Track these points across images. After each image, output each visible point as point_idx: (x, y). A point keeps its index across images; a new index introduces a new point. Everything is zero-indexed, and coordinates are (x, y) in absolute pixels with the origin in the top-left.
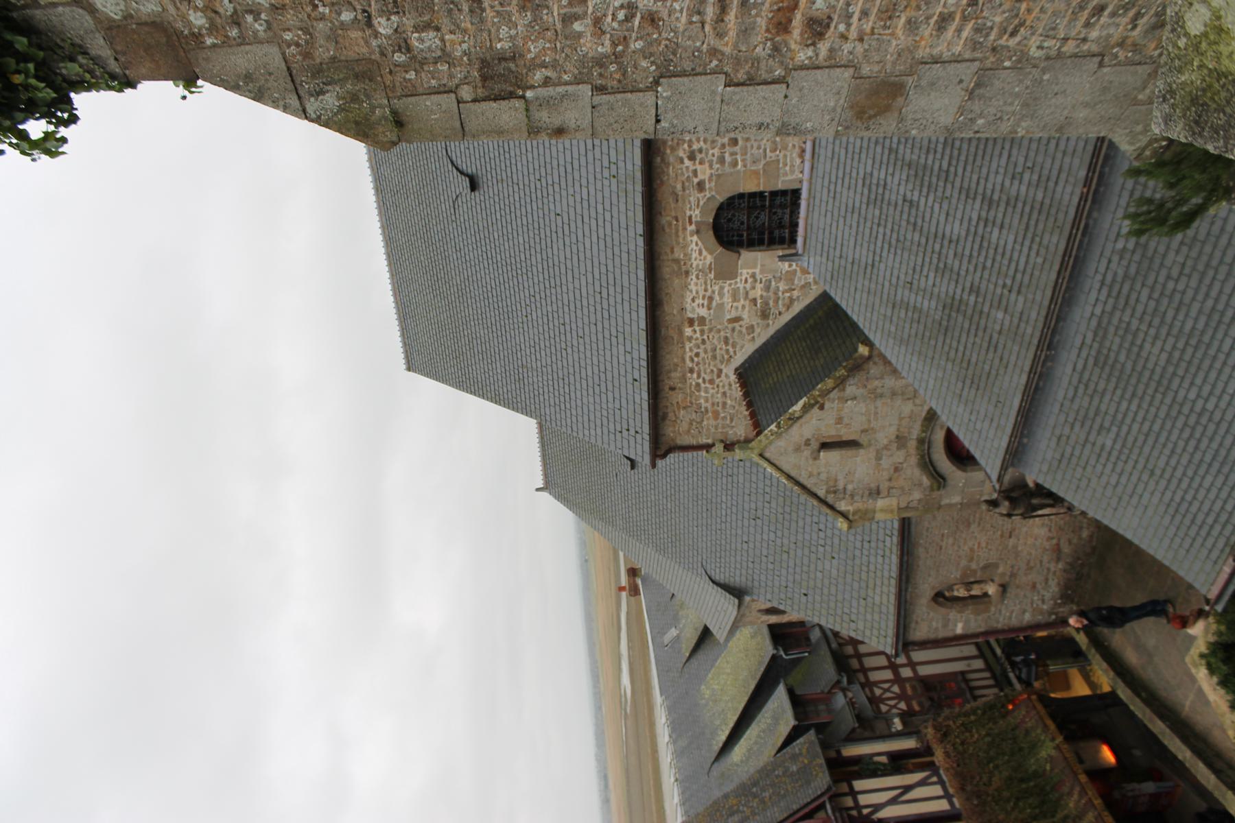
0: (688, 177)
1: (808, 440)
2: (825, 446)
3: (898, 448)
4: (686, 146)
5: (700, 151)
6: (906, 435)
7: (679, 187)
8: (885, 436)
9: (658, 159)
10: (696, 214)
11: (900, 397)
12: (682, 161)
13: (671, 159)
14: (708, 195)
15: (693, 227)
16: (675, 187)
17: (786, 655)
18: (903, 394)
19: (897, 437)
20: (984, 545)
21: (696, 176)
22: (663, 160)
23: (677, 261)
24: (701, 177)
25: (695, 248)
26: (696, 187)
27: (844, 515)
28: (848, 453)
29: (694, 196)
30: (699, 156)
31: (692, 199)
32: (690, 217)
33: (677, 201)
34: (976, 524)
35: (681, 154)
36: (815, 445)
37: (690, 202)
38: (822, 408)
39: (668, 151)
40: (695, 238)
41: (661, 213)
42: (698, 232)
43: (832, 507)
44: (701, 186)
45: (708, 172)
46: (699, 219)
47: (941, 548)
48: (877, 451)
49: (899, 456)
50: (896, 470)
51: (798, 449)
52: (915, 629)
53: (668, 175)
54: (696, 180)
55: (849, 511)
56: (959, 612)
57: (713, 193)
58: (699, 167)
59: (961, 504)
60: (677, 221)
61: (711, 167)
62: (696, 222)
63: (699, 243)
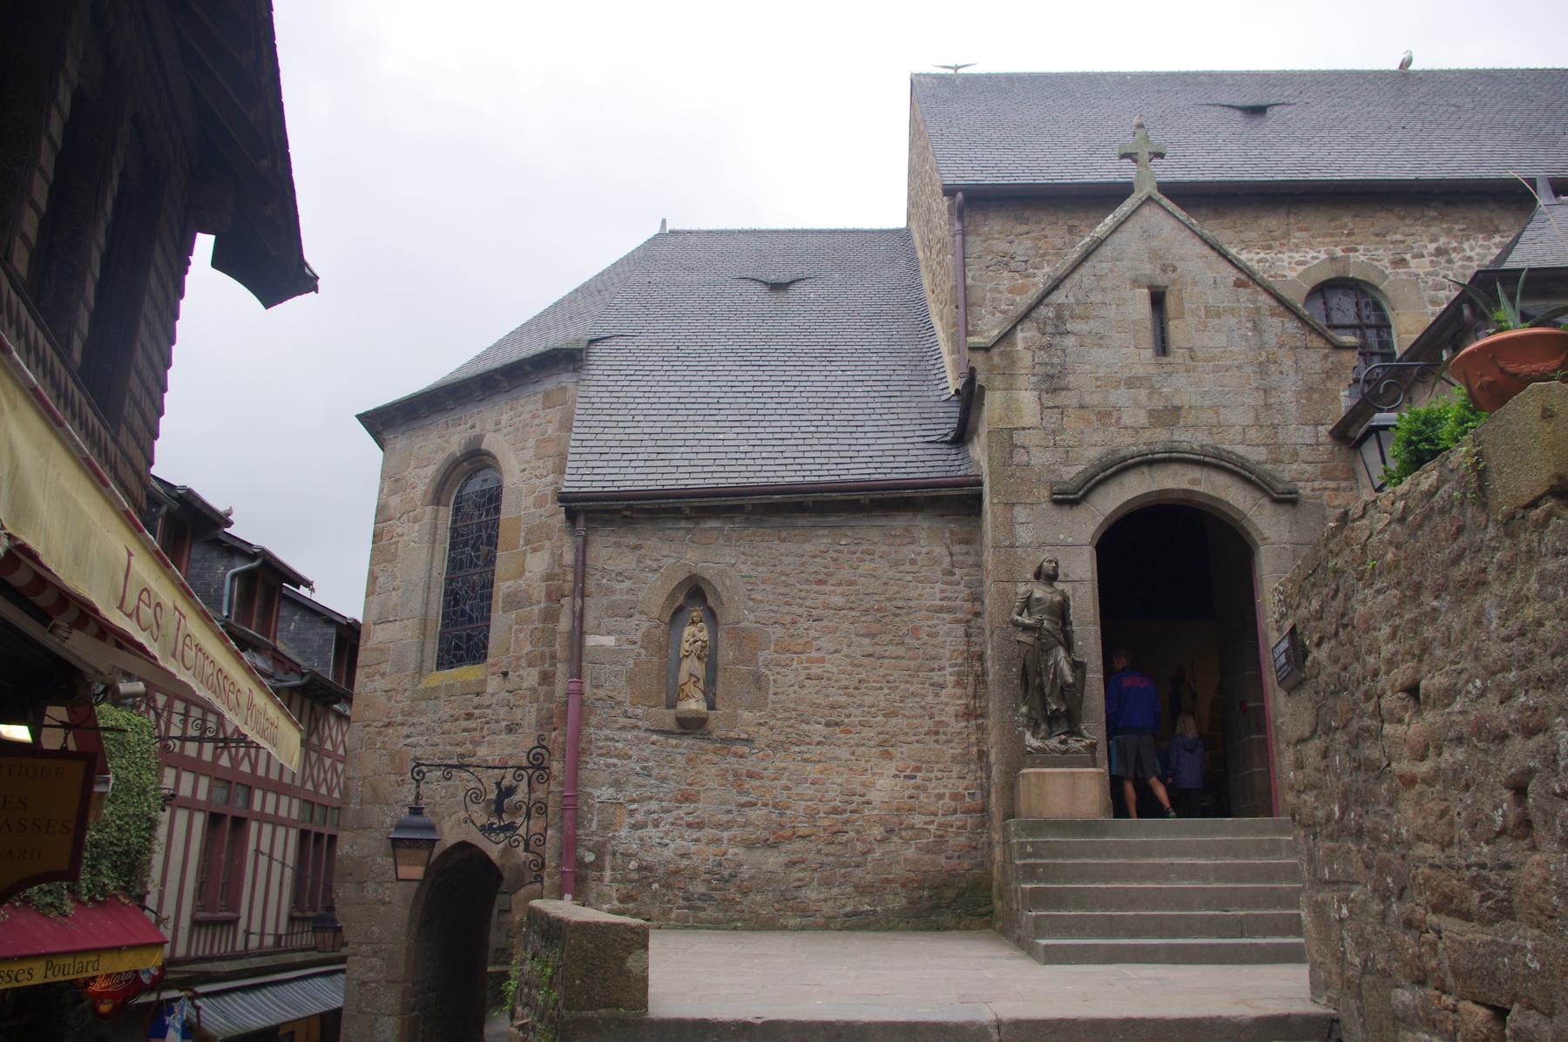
0: (1412, 248)
1: (1175, 269)
2: (1158, 299)
3: (1151, 413)
4: (1455, 244)
5: (1450, 261)
6: (1182, 423)
7: (1398, 237)
8: (1180, 388)
9: (1433, 214)
10: (1360, 257)
11: (1261, 403)
12: (1432, 241)
13: (1434, 229)
14: (1387, 272)
15: (1339, 252)
16: (1396, 233)
17: (234, 576)
18: (1267, 406)
19: (1178, 409)
20: (815, 671)
21: (1414, 257)
22: (1434, 219)
23: (1287, 235)
24: (1413, 263)
25: (1309, 256)
26: (1398, 257)
27: (1006, 337)
28: (1147, 335)
29: (1384, 257)
30: (1442, 260)
31: (1381, 251)
32: (1356, 250)
33: (1377, 235)
34: (870, 650)
35: (1442, 240)
36: (1161, 280)
37: (1376, 249)
38: (1238, 284)
39: (1445, 226)
40: (1323, 256)
41: (1357, 216)
42: (1333, 259)
43: (1025, 316)
44: (1400, 262)
45: (1420, 271)
46: (1352, 260)
47: (821, 582)
48: (1148, 378)
49: (1135, 417)
50: (1104, 415)
51: (1154, 254)
52: (618, 545)
53: (1412, 226)
54: (1408, 257)
55: (1014, 344)
56: (647, 636)
57: (1391, 278)
58: (1427, 260)
59: (1012, 546)
60: (1348, 235)
61: (1428, 274)
62: (1348, 257)
63: (1317, 261)
